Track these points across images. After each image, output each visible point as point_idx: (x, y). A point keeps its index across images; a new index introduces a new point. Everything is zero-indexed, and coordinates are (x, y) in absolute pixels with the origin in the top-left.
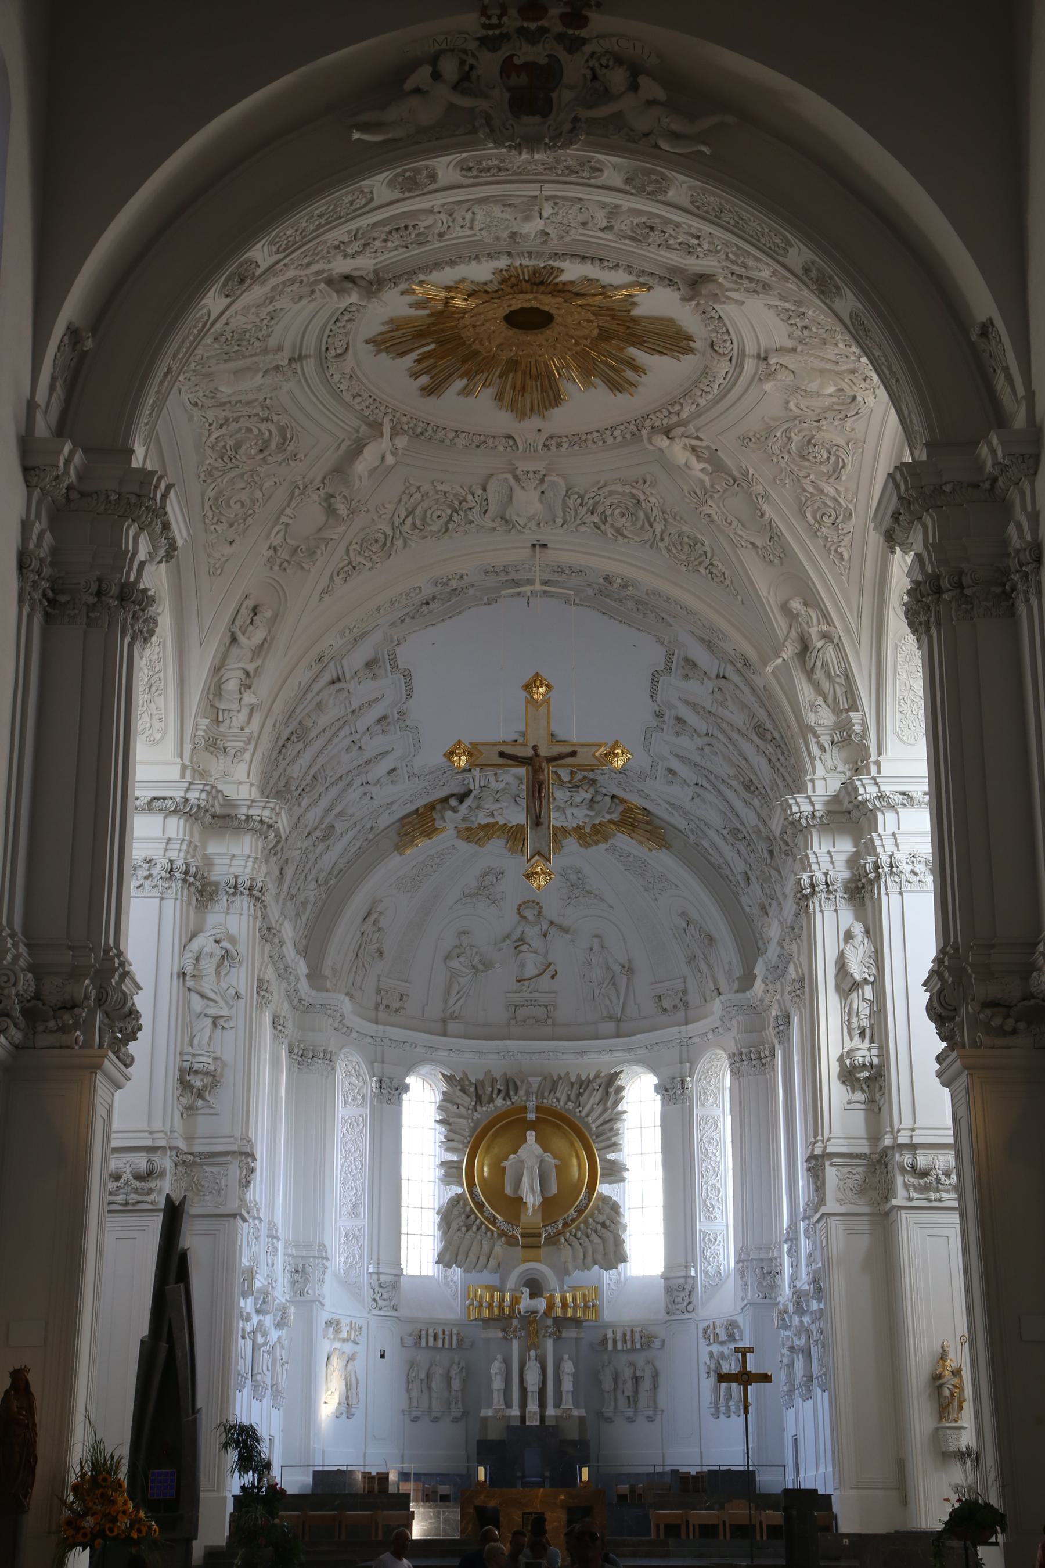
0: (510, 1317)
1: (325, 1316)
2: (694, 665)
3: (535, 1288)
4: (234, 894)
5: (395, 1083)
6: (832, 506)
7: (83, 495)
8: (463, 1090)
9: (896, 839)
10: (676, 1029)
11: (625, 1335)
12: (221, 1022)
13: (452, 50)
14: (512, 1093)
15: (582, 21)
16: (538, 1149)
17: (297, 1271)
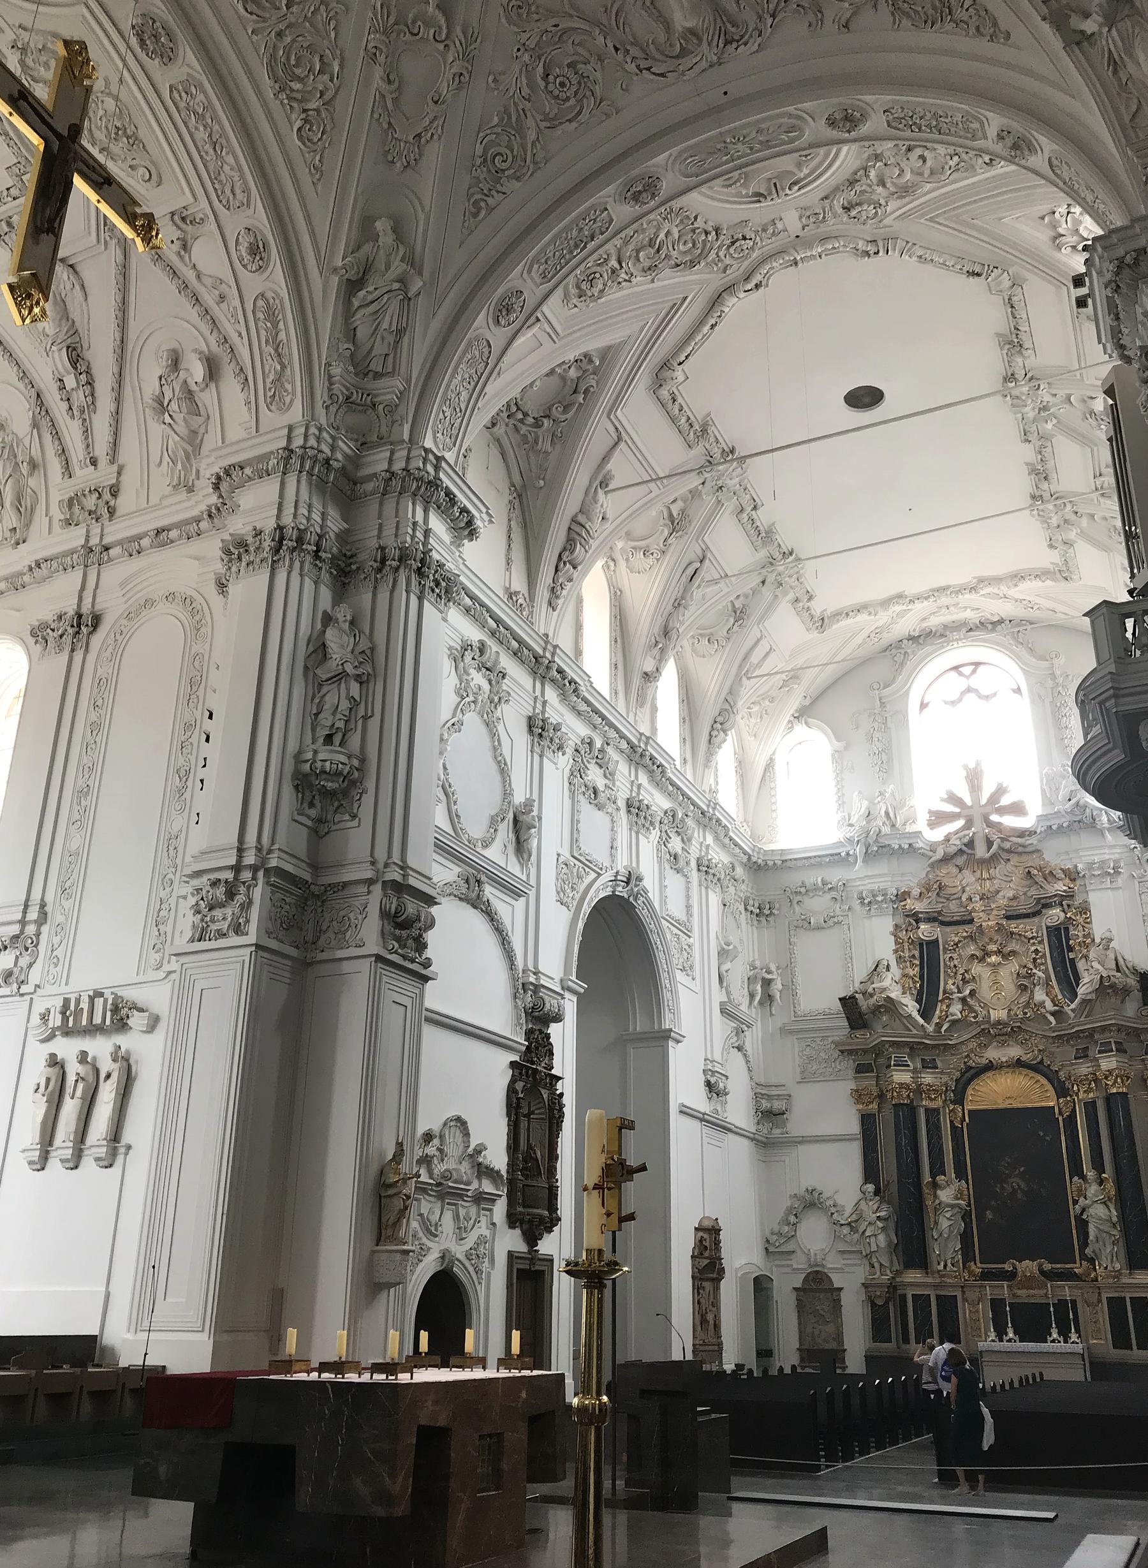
6: (515, 153)
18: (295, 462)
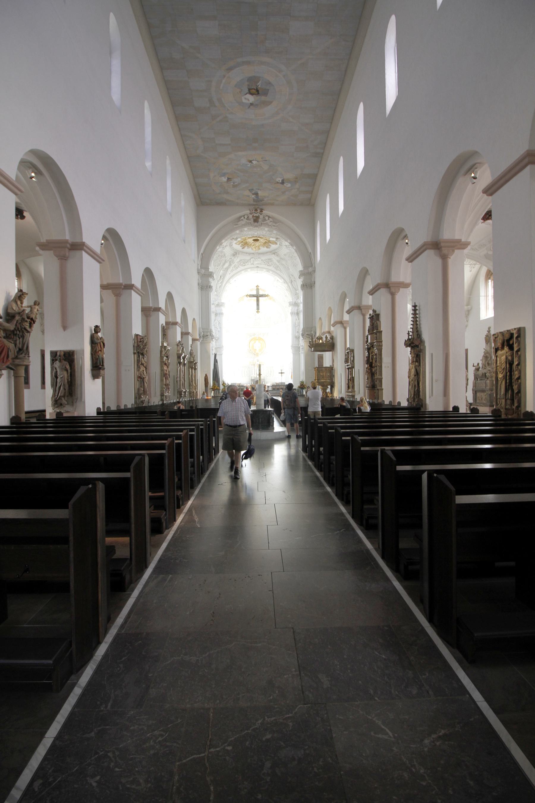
7: (204, 275)
13: (246, 215)
15: (262, 212)
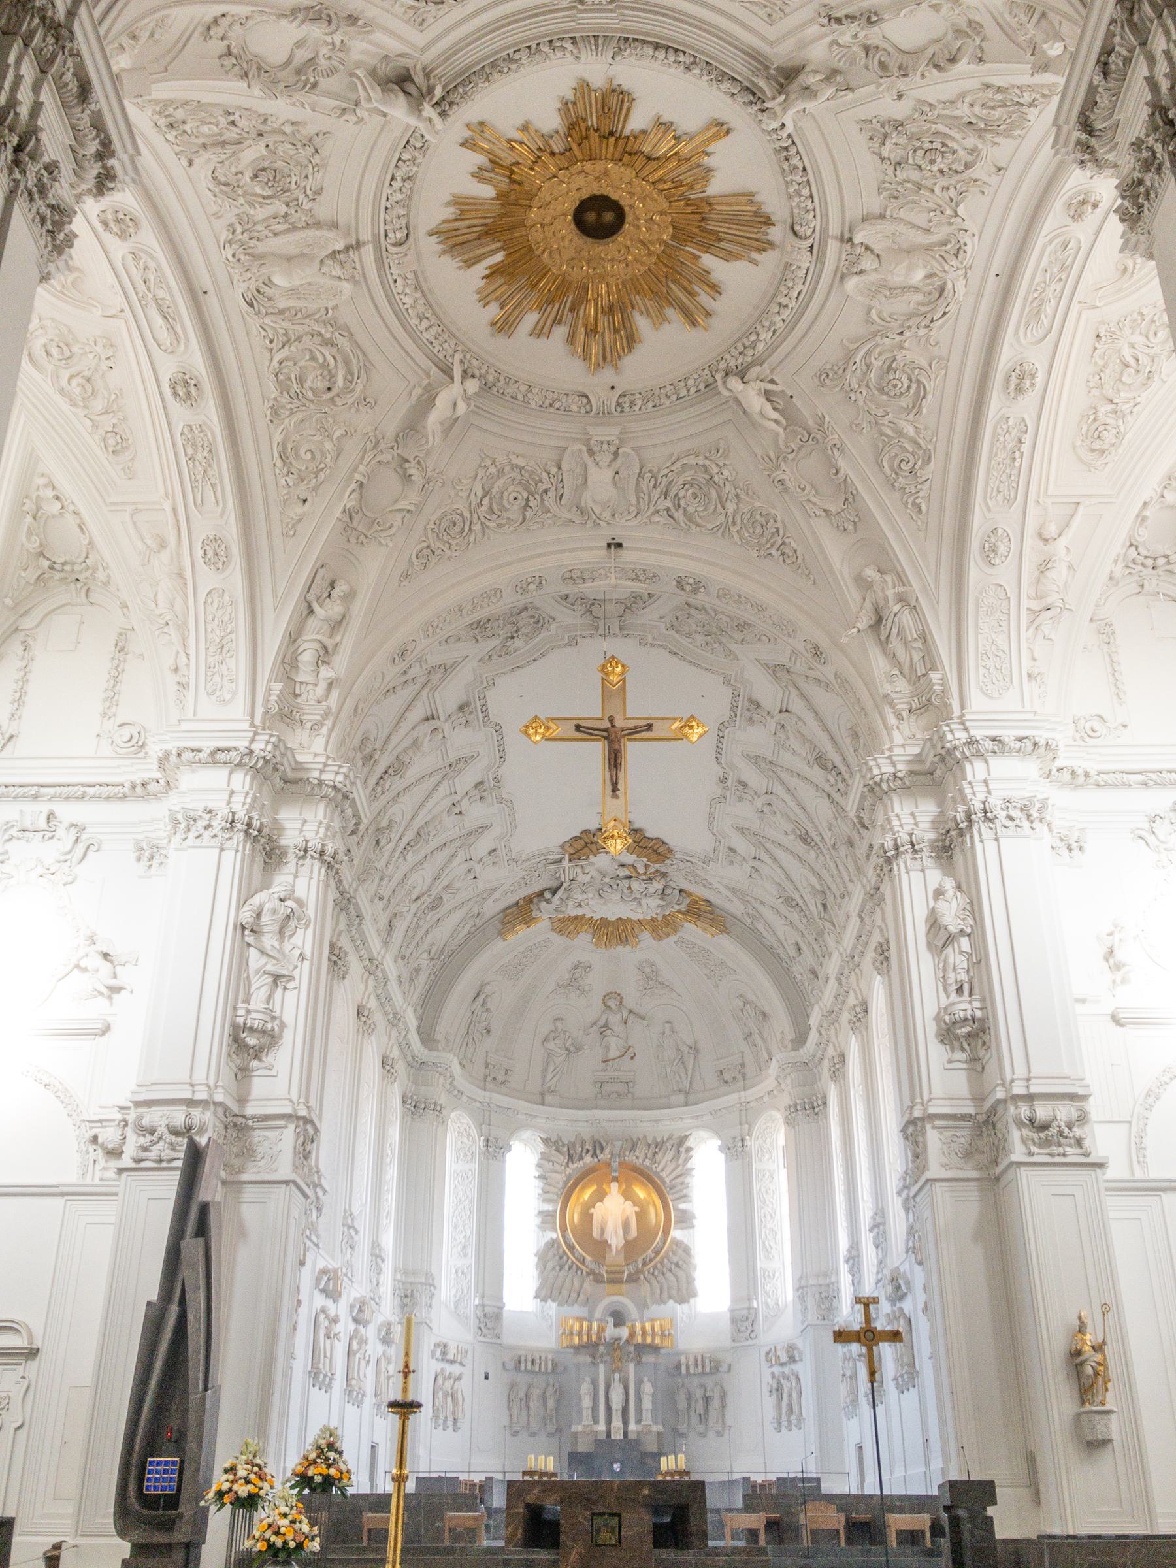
0: (597, 1345)
1: (434, 1340)
2: (758, 706)
3: (619, 1318)
4: (303, 857)
5: (500, 1143)
8: (558, 1150)
9: (987, 786)
10: (736, 1095)
11: (696, 1361)
12: (281, 983)
14: (598, 1152)
16: (622, 1199)
17: (406, 1296)
18: (877, 789)
